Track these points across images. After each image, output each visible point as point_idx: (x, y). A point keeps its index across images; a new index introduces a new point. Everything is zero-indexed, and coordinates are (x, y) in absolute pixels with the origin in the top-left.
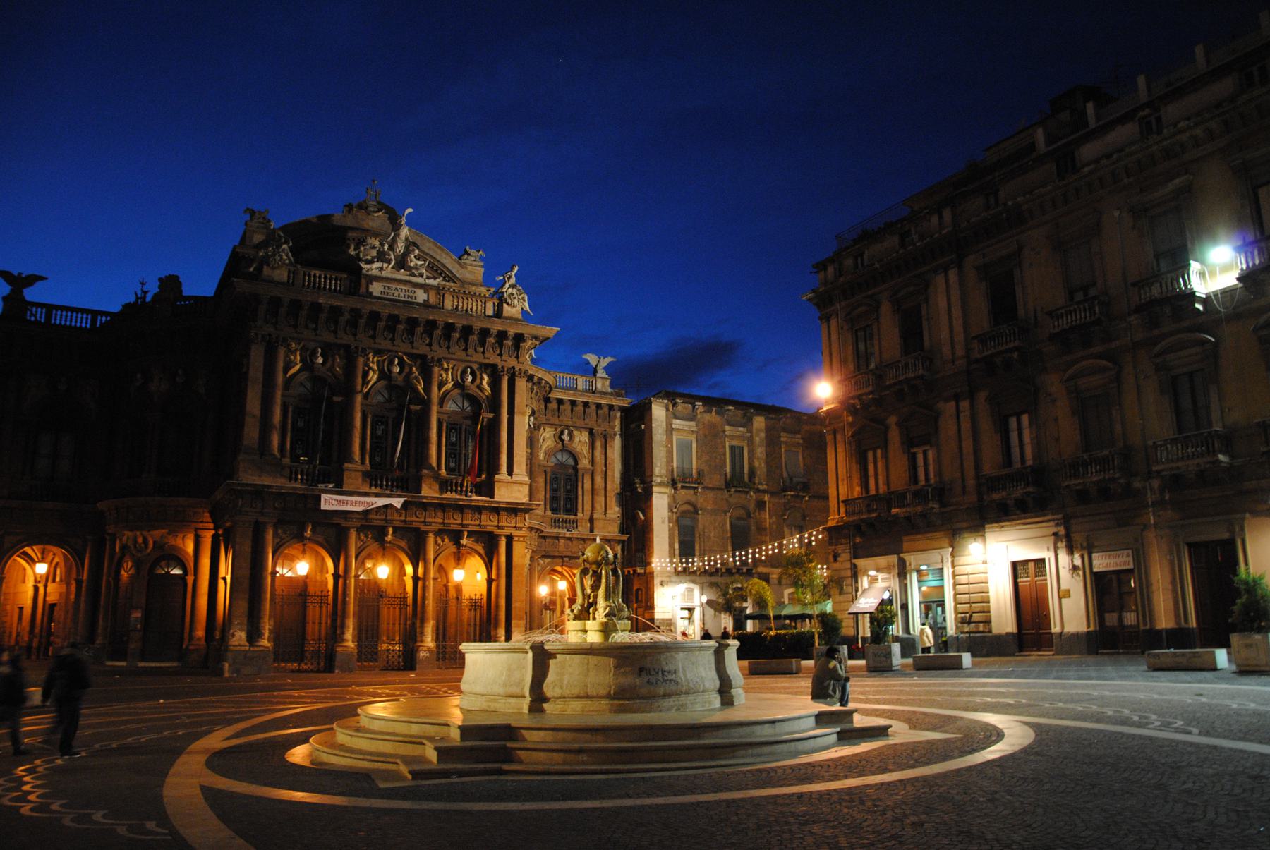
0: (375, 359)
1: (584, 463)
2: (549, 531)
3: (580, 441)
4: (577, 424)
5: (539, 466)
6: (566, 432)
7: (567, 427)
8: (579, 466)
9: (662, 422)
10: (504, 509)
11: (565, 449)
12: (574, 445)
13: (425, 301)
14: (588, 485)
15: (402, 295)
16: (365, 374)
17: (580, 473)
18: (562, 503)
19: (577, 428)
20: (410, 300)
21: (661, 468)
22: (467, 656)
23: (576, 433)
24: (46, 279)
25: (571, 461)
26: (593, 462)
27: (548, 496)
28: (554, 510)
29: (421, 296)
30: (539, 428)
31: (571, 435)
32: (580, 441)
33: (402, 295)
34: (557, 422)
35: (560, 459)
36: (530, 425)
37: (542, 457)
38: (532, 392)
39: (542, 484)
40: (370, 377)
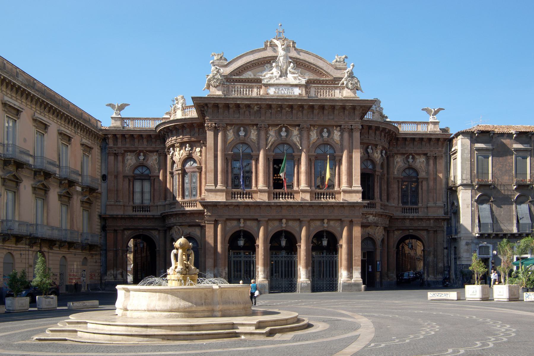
0: (273, 130)
1: (422, 174)
2: (398, 214)
3: (420, 162)
4: (418, 152)
5: (394, 178)
6: (411, 157)
7: (411, 154)
8: (420, 176)
9: (468, 146)
10: (346, 206)
11: (410, 168)
12: (416, 164)
13: (300, 94)
14: (425, 187)
15: (286, 92)
16: (267, 139)
17: (420, 180)
18: (409, 199)
19: (419, 154)
20: (291, 94)
21: (467, 174)
22: (118, 291)
23: (417, 157)
24: (130, 105)
25: (414, 174)
26: (428, 173)
27: (400, 195)
28: (404, 203)
29: (297, 92)
30: (393, 156)
31: (413, 158)
32: (420, 162)
33: (286, 92)
34: (404, 152)
35: (408, 174)
36: (382, 155)
37: (396, 173)
38: (381, 136)
39: (397, 189)
40: (269, 140)
